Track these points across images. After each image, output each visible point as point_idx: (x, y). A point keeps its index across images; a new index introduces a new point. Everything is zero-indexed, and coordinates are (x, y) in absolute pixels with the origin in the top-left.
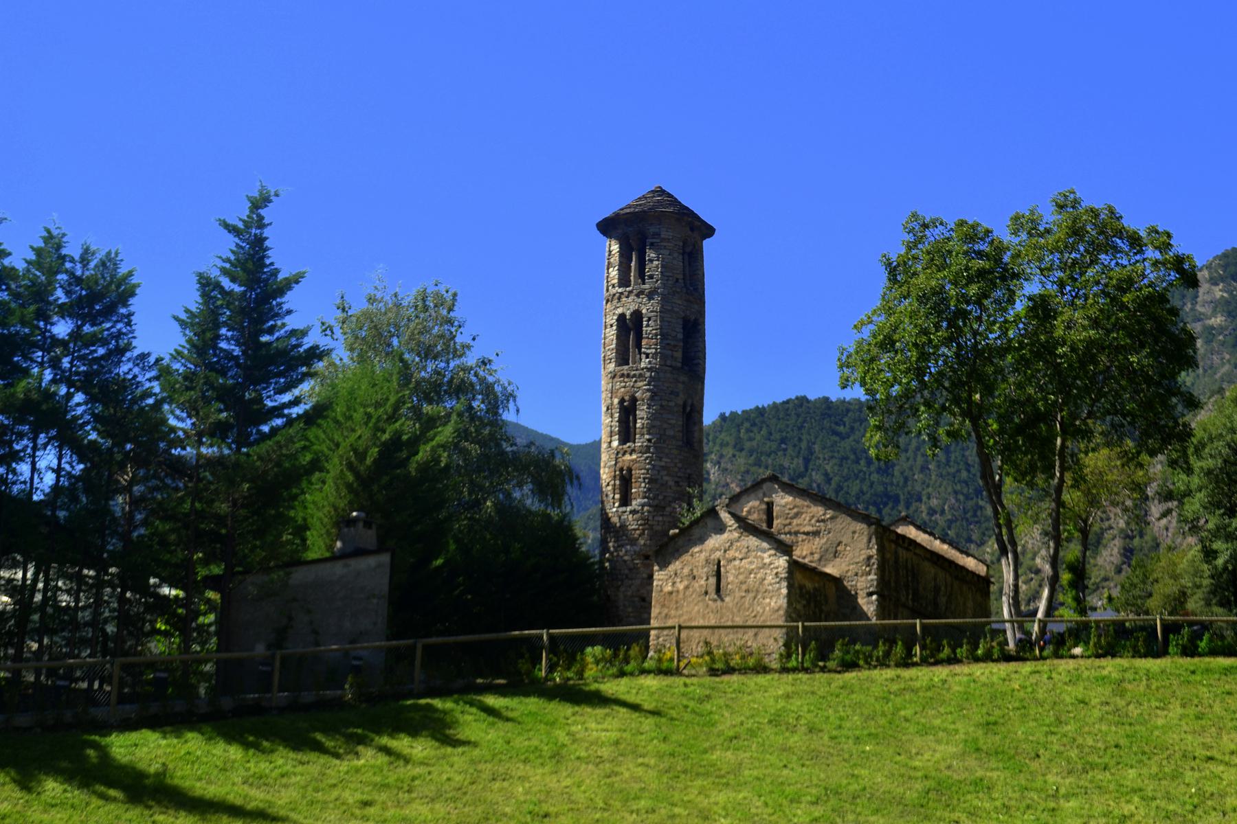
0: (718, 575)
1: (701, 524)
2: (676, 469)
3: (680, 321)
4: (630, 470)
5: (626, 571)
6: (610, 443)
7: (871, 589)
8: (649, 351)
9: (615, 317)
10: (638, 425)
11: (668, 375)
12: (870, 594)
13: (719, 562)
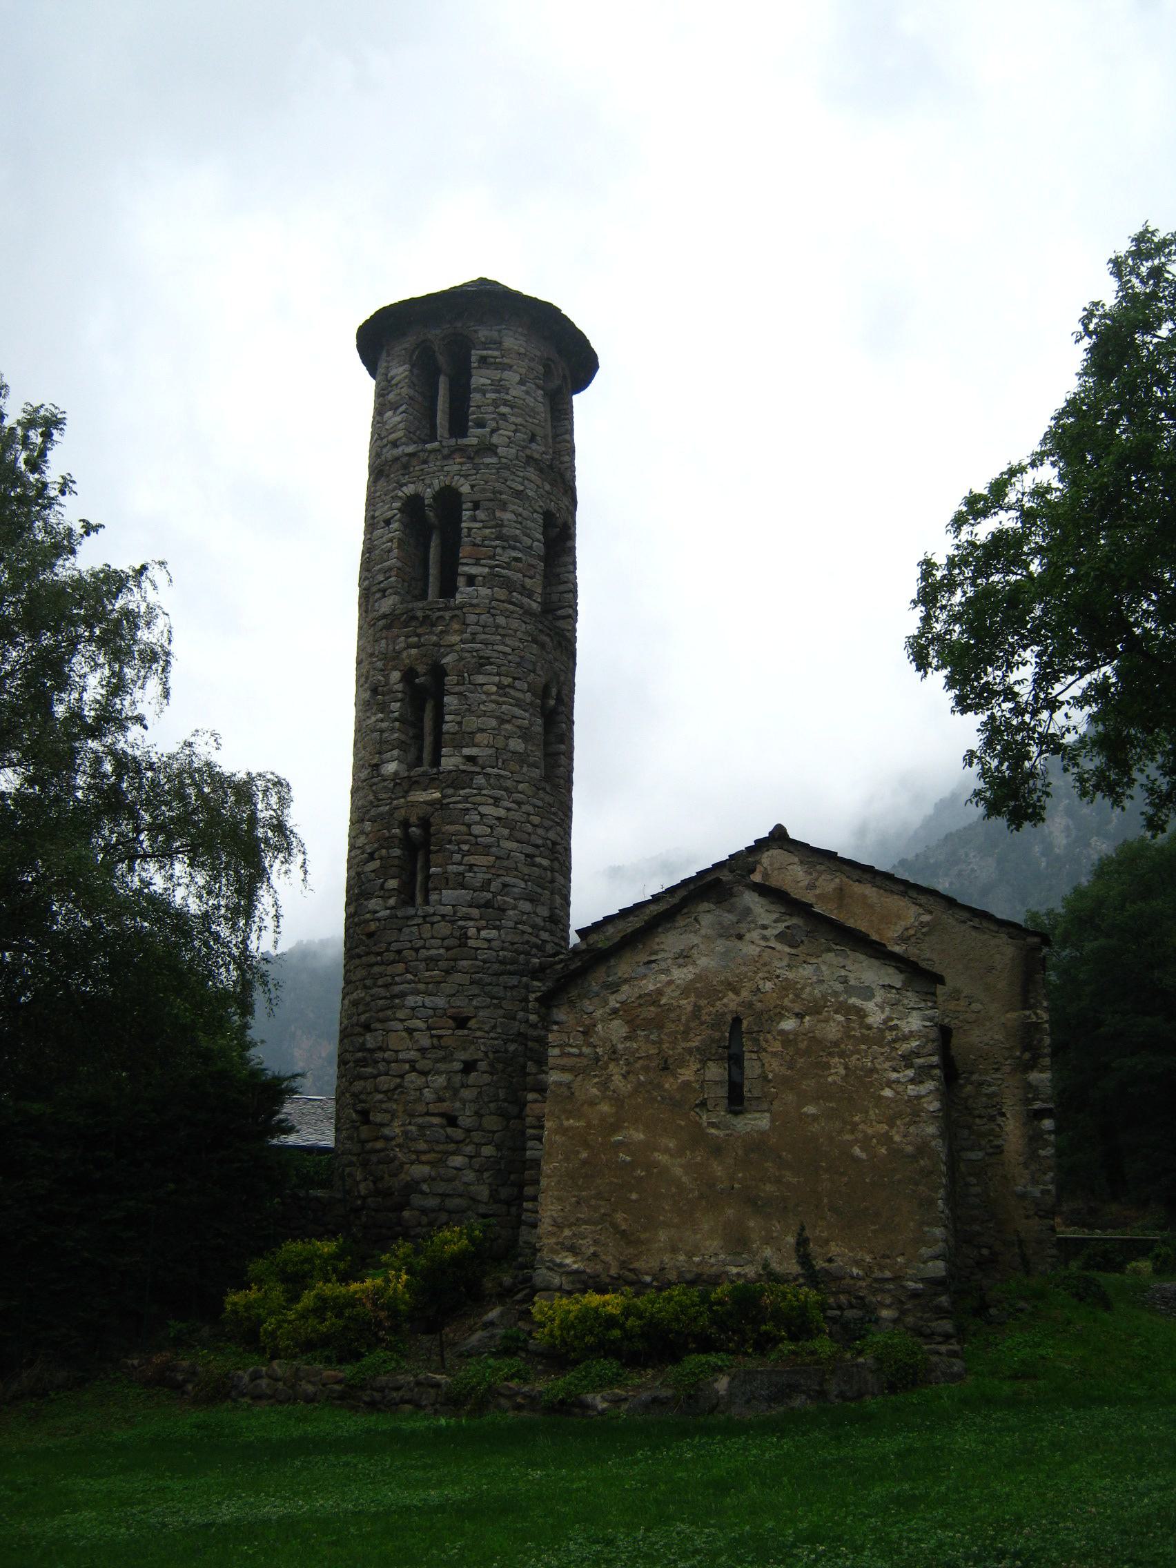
0: (735, 1060)
1: (681, 922)
2: (529, 828)
3: (539, 518)
4: (425, 823)
5: (412, 1055)
6: (376, 767)
7: (1037, 1105)
8: (474, 570)
9: (397, 505)
10: (446, 727)
11: (515, 624)
12: (1039, 1115)
13: (737, 1021)
